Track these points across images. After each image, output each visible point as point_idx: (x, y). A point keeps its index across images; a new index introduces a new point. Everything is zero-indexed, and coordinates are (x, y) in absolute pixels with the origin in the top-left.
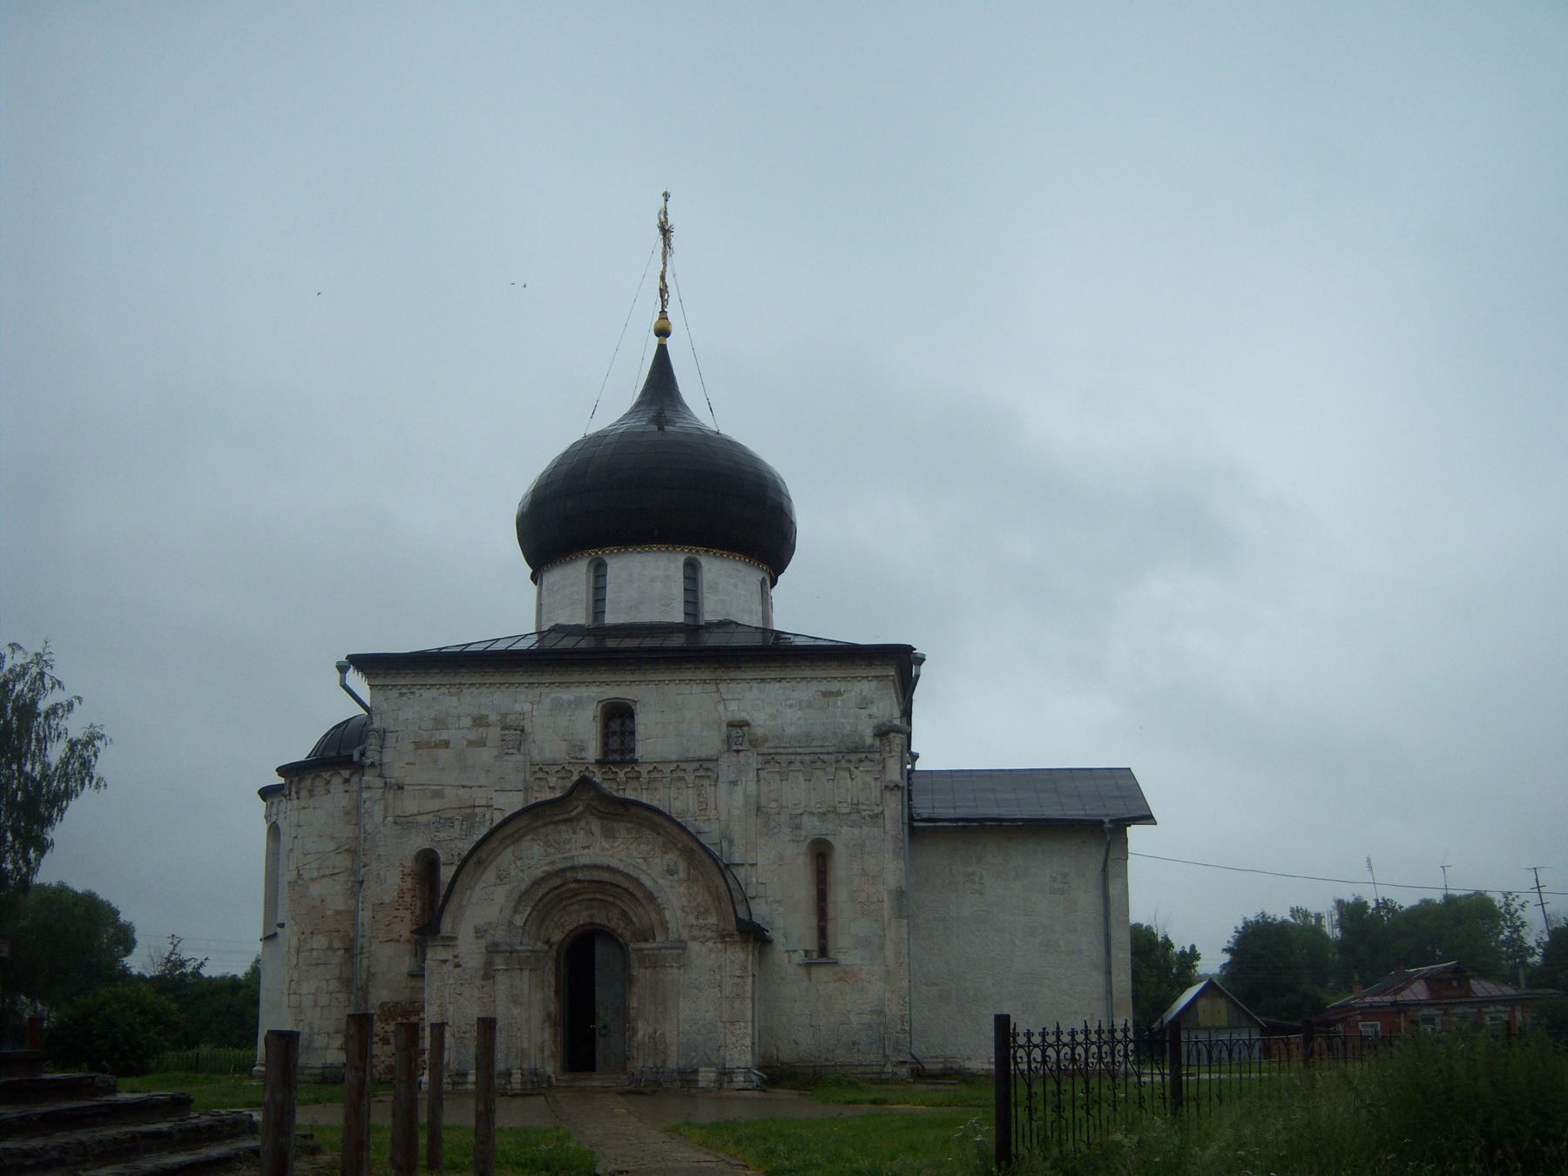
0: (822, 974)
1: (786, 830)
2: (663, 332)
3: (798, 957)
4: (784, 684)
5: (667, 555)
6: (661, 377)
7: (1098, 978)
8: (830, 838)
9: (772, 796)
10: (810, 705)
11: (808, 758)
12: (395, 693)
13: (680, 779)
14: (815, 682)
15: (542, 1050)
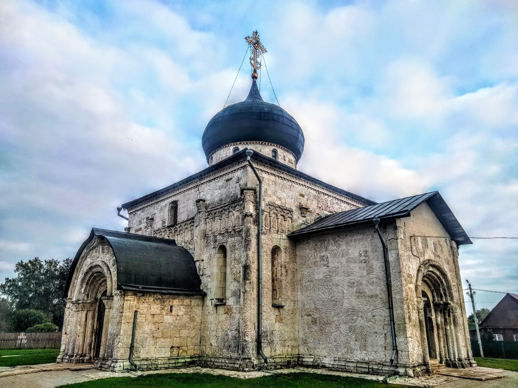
0: (221, 310)
1: (212, 243)
2: (254, 77)
3: (214, 302)
4: (216, 180)
5: (227, 148)
6: (254, 92)
7: (385, 312)
8: (225, 244)
9: (210, 229)
10: (222, 187)
11: (220, 210)
12: (133, 215)
13: (187, 228)
14: (224, 177)
15: (91, 345)
